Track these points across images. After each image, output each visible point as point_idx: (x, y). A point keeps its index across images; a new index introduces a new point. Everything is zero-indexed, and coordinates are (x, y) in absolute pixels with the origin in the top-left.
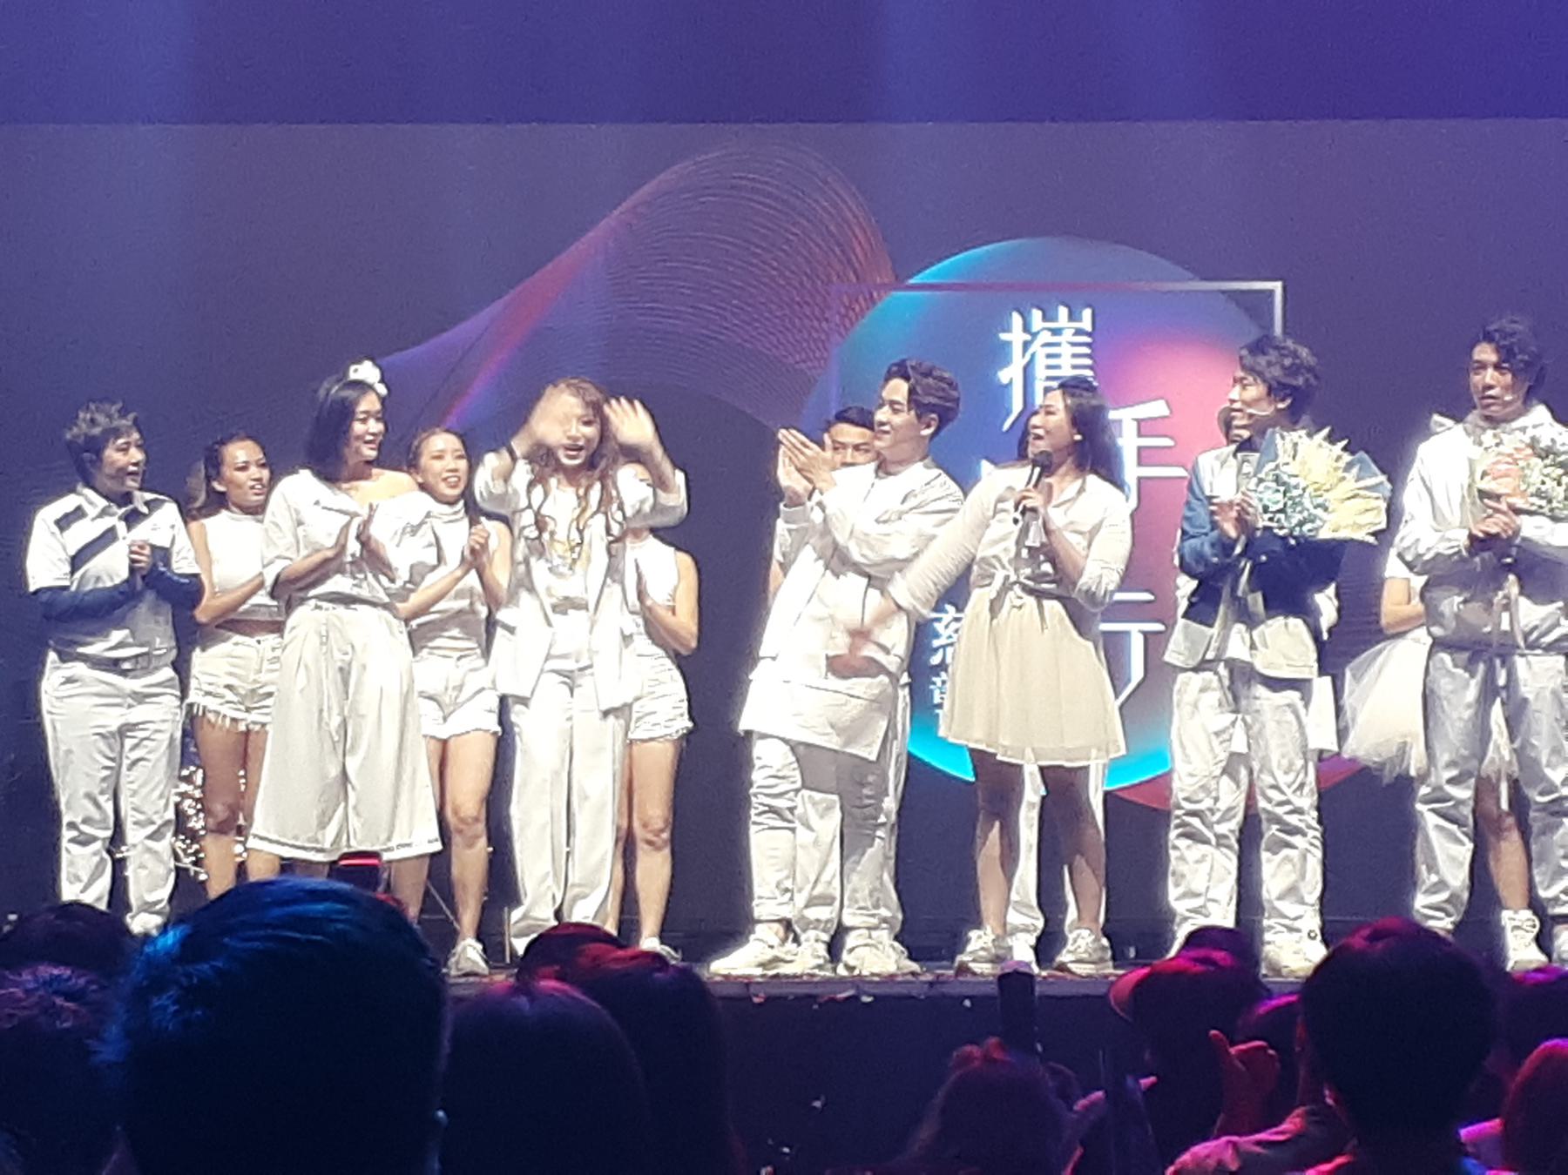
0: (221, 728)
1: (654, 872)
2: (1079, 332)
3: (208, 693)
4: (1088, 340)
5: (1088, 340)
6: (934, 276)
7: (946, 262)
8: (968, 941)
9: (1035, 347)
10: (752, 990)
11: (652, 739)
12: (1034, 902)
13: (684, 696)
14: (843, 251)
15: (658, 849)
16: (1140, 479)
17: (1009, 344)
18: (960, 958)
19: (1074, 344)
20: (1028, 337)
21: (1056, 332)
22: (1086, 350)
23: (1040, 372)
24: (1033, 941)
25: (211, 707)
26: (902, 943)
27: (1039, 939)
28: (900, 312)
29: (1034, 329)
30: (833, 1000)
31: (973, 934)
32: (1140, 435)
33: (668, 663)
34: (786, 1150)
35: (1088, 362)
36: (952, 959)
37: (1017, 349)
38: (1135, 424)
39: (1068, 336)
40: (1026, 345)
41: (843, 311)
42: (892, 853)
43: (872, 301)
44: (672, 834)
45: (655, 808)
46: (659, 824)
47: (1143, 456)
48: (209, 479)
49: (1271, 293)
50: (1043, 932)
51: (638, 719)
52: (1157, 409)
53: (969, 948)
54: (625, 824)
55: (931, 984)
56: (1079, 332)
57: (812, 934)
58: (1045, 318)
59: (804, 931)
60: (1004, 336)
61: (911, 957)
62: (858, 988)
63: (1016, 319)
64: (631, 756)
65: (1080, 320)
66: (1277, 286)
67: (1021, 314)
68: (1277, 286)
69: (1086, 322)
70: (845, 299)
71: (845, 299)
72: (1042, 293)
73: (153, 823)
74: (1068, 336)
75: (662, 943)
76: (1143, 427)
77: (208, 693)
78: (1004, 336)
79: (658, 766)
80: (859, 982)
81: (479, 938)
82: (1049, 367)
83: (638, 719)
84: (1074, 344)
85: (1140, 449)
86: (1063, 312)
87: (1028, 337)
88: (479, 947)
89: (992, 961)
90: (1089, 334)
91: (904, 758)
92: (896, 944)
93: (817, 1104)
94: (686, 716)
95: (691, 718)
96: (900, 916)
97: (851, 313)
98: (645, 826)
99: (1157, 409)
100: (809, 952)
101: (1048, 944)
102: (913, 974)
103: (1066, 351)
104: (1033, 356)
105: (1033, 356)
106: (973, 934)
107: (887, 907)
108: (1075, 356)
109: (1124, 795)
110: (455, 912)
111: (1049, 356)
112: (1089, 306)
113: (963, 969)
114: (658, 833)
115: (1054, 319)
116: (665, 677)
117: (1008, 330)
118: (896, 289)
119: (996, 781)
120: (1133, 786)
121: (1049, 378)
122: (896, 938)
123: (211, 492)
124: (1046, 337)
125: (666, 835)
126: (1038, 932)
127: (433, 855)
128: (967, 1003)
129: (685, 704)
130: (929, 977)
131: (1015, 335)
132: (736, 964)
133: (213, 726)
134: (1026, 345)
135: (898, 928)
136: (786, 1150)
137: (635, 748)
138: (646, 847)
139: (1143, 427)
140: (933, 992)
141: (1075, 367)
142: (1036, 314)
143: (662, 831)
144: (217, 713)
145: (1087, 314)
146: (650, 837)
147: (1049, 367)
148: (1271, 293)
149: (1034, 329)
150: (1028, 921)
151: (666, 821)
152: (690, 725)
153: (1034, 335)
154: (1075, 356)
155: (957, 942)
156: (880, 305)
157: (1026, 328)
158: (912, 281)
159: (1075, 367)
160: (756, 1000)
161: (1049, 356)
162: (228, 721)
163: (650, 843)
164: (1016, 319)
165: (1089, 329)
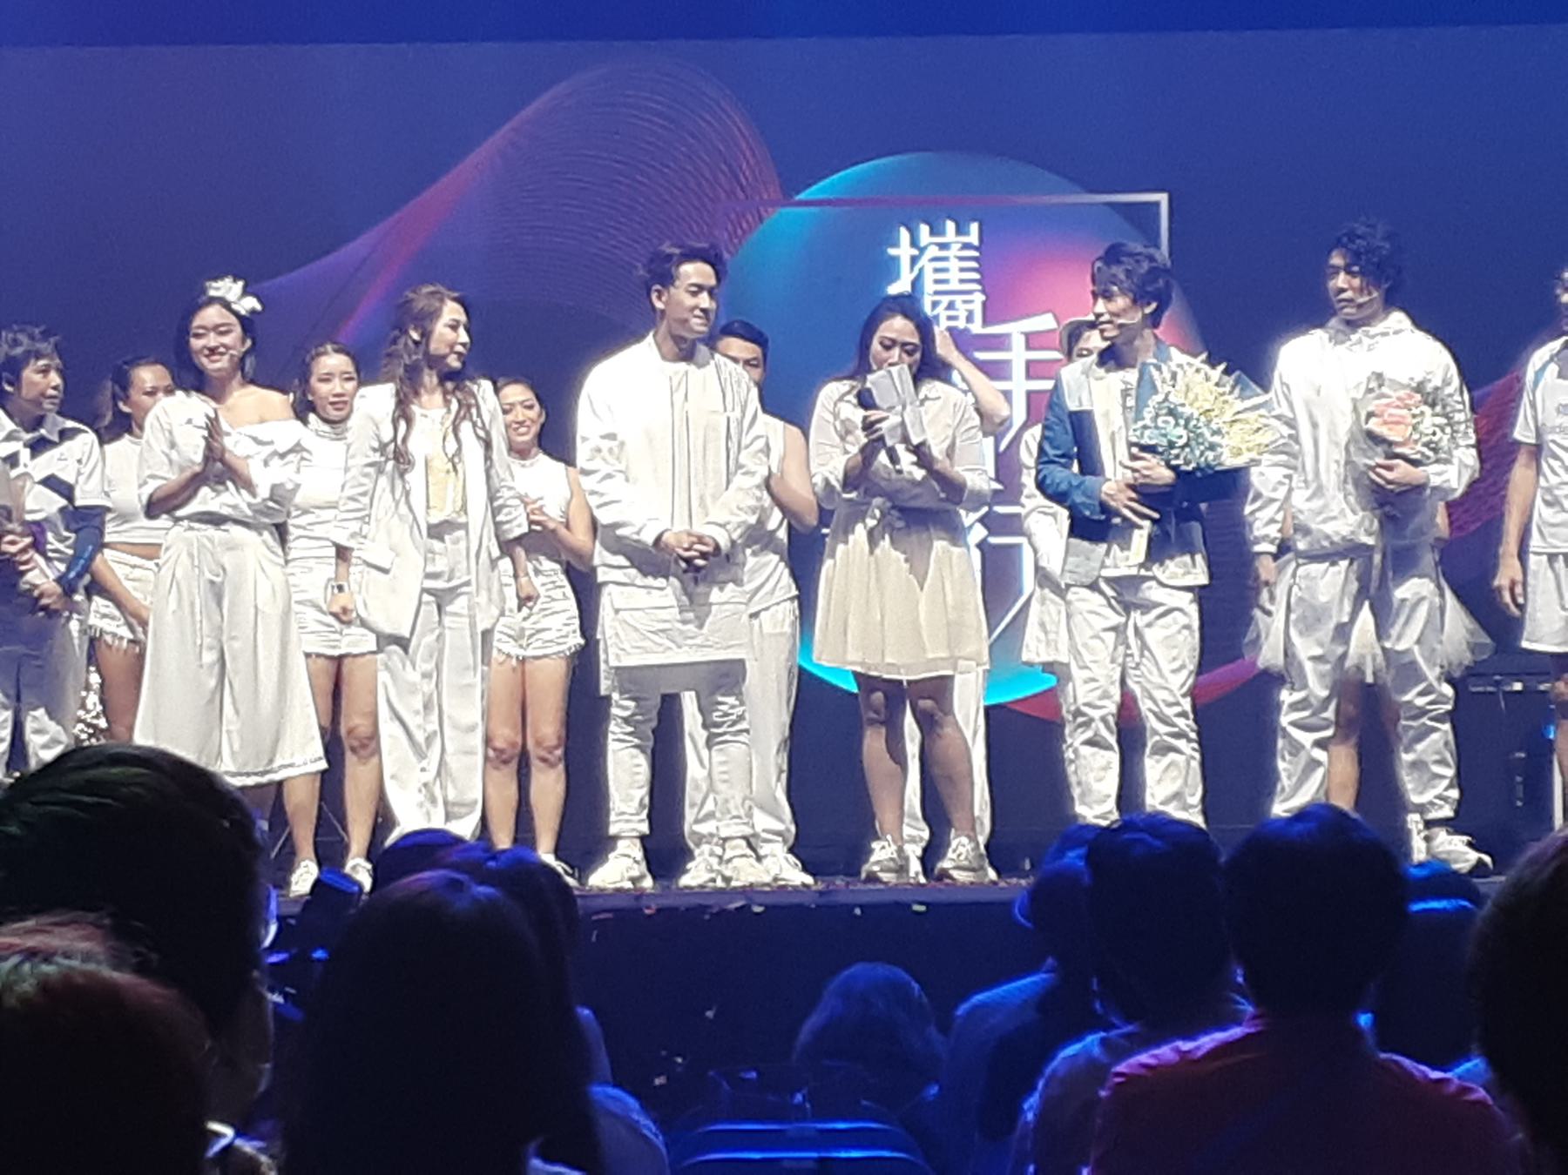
0: (118, 650)
1: (548, 788)
2: (966, 246)
3: (104, 616)
4: (976, 254)
5: (976, 254)
6: (820, 190)
7: (835, 177)
8: (870, 852)
9: (924, 261)
10: (644, 902)
11: (546, 656)
12: (919, 814)
13: (576, 613)
14: (730, 166)
15: (552, 765)
16: (1029, 394)
17: (896, 259)
18: (865, 868)
19: (962, 259)
20: (915, 252)
21: (943, 246)
22: (974, 264)
23: (929, 287)
24: (919, 852)
25: (108, 629)
26: (797, 856)
27: (925, 850)
28: (787, 228)
29: (922, 244)
30: (723, 912)
31: (875, 845)
32: (1029, 347)
33: (563, 580)
34: (679, 1060)
35: (976, 276)
36: (859, 873)
37: (905, 264)
38: (1022, 339)
39: (955, 250)
40: (914, 260)
41: (730, 227)
42: (785, 767)
43: (761, 219)
44: (566, 753)
45: (548, 726)
46: (554, 742)
47: (1032, 370)
48: (115, 397)
49: (1157, 204)
50: (930, 843)
51: (531, 636)
52: (1045, 322)
53: (873, 859)
54: (519, 740)
55: (821, 893)
56: (966, 246)
57: (705, 848)
58: (933, 233)
59: (698, 845)
60: (892, 251)
61: (805, 869)
62: (747, 898)
63: (904, 234)
64: (523, 673)
65: (967, 233)
66: (1162, 198)
67: (909, 229)
68: (1162, 198)
69: (973, 238)
70: (733, 216)
71: (733, 216)
72: (932, 210)
73: (60, 742)
74: (955, 250)
75: (558, 858)
76: (1032, 341)
77: (104, 616)
78: (892, 251)
79: (550, 681)
80: (748, 891)
81: (369, 858)
82: (937, 282)
83: (531, 636)
84: (962, 259)
85: (1029, 364)
86: (950, 226)
87: (915, 252)
88: (369, 866)
89: (896, 871)
90: (976, 248)
91: (796, 671)
92: (792, 858)
93: (710, 1014)
94: (578, 633)
95: (583, 634)
96: (793, 829)
97: (739, 232)
98: (538, 743)
99: (1045, 322)
100: (702, 866)
101: (931, 854)
102: (804, 885)
103: (954, 265)
104: (921, 270)
105: (921, 270)
106: (875, 845)
107: (781, 820)
108: (962, 270)
109: (1018, 708)
110: (345, 828)
111: (936, 270)
112: (974, 220)
113: (873, 878)
114: (550, 750)
115: (942, 233)
116: (557, 594)
117: (896, 244)
118: (784, 206)
119: (889, 698)
120: (1025, 699)
121: (937, 293)
122: (791, 850)
123: (118, 413)
124: (933, 251)
125: (559, 752)
126: (924, 844)
127: (323, 773)
128: (858, 911)
129: (577, 622)
130: (820, 886)
131: (903, 250)
132: (695, 876)
133: (109, 647)
134: (914, 260)
135: (791, 840)
136: (679, 1060)
137: (528, 666)
138: (542, 765)
139: (1032, 341)
140: (822, 901)
141: (962, 281)
142: (924, 229)
143: (556, 747)
144: (114, 635)
145: (974, 227)
146: (543, 754)
147: (937, 282)
148: (1157, 204)
149: (922, 244)
150: (914, 833)
151: (559, 738)
152: (582, 642)
153: (922, 250)
154: (962, 270)
155: (864, 853)
156: (767, 222)
157: (914, 243)
158: (802, 196)
159: (962, 281)
160: (647, 912)
161: (936, 270)
162: (125, 643)
163: (544, 760)
164: (904, 234)
165: (976, 242)
